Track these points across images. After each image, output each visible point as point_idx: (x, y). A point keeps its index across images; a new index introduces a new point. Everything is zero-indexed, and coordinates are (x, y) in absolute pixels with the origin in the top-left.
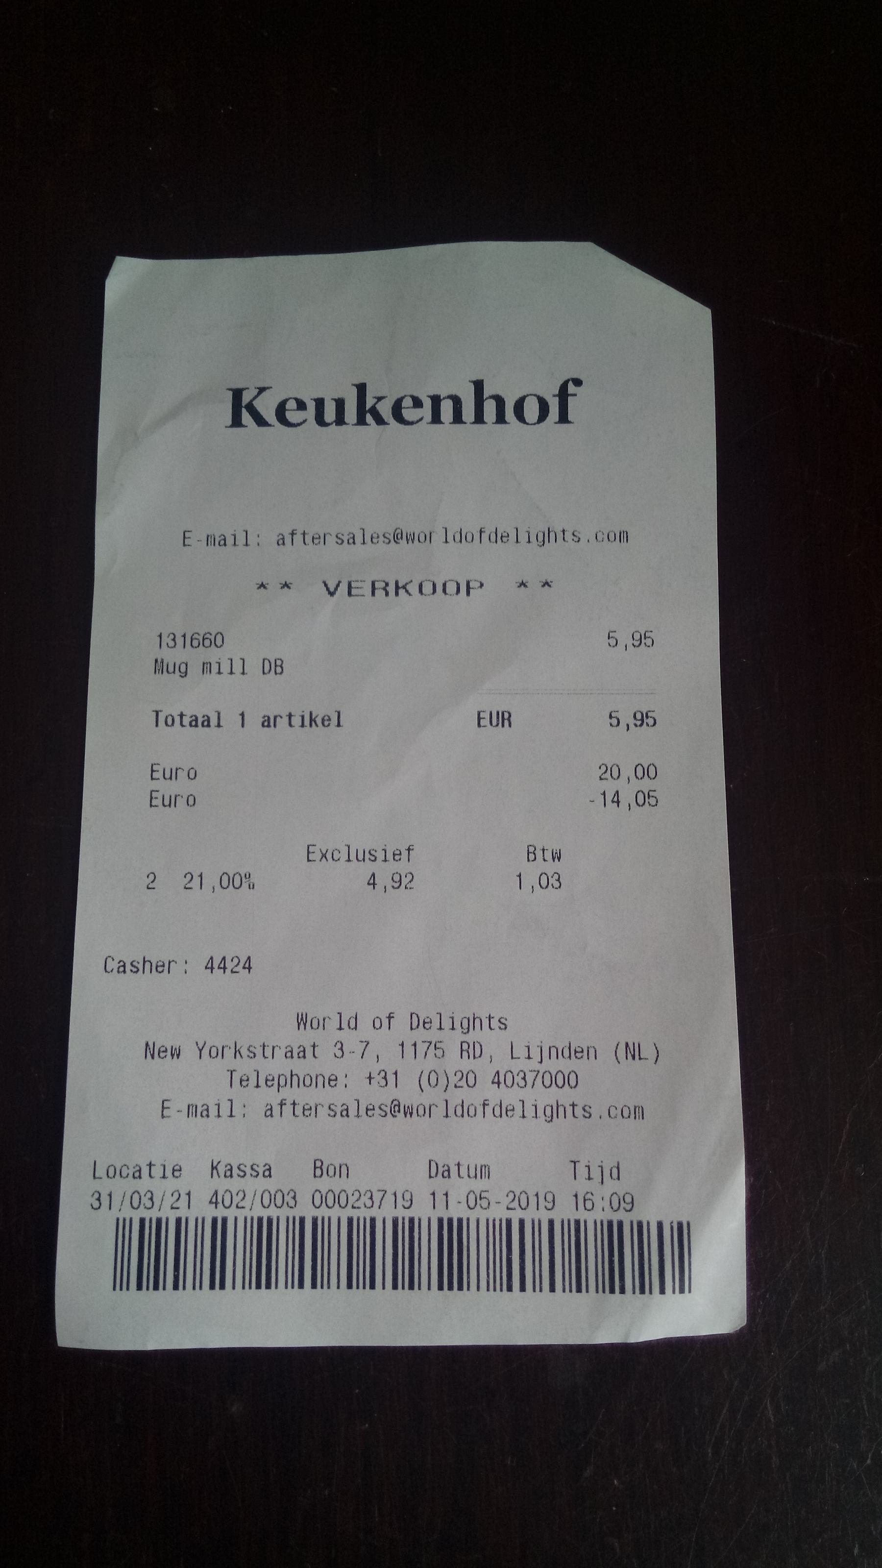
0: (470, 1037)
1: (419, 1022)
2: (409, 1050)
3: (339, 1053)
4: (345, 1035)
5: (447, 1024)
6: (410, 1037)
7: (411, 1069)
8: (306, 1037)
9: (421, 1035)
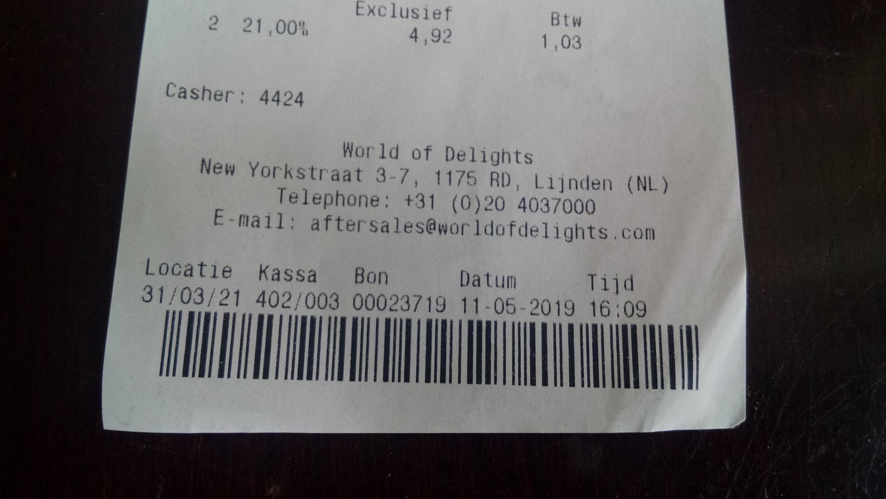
0: (500, 169)
1: (453, 155)
2: (444, 178)
3: (381, 178)
4: (388, 164)
5: (479, 157)
6: (445, 167)
7: (446, 194)
8: (351, 163)
9: (454, 165)
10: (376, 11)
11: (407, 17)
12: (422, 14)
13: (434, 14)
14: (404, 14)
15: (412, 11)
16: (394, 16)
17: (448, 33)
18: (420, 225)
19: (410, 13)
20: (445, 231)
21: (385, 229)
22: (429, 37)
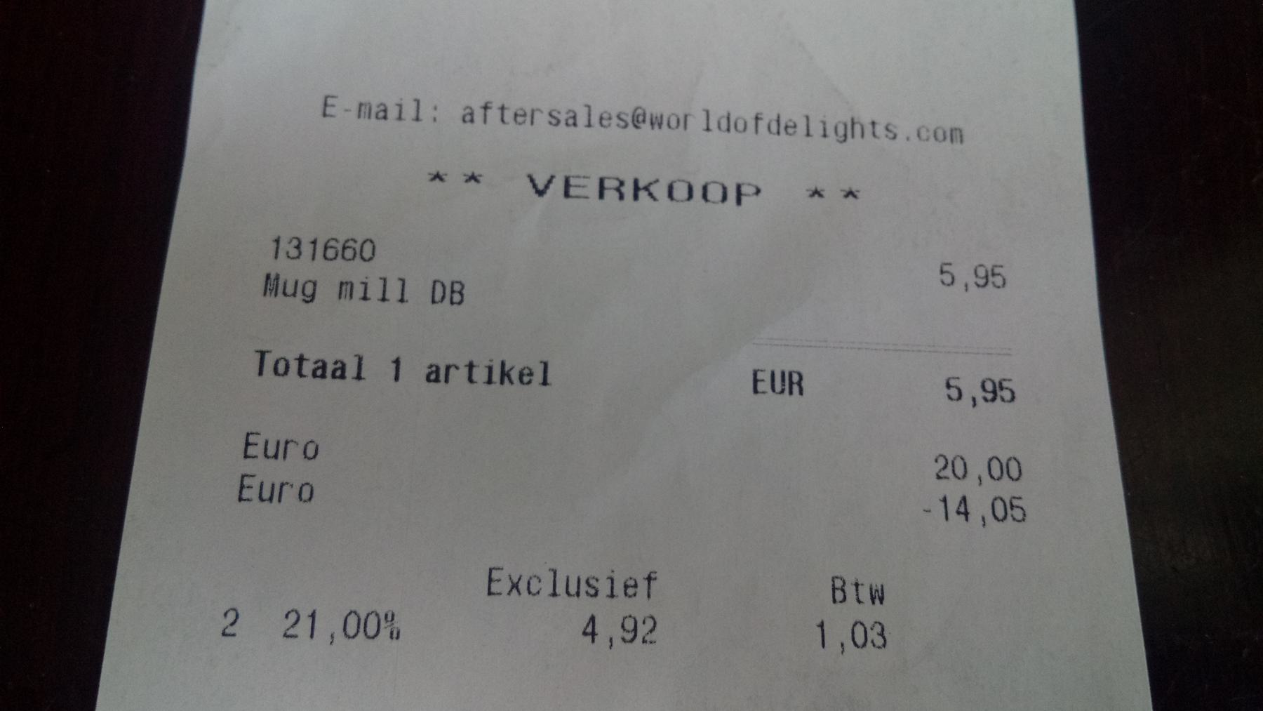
10: (523, 586)
11: (578, 594)
12: (604, 587)
13: (626, 587)
14: (573, 590)
15: (587, 582)
16: (554, 594)
17: (650, 623)
18: (623, 116)
19: (584, 587)
20: (660, 125)
21: (571, 121)
22: (618, 633)
